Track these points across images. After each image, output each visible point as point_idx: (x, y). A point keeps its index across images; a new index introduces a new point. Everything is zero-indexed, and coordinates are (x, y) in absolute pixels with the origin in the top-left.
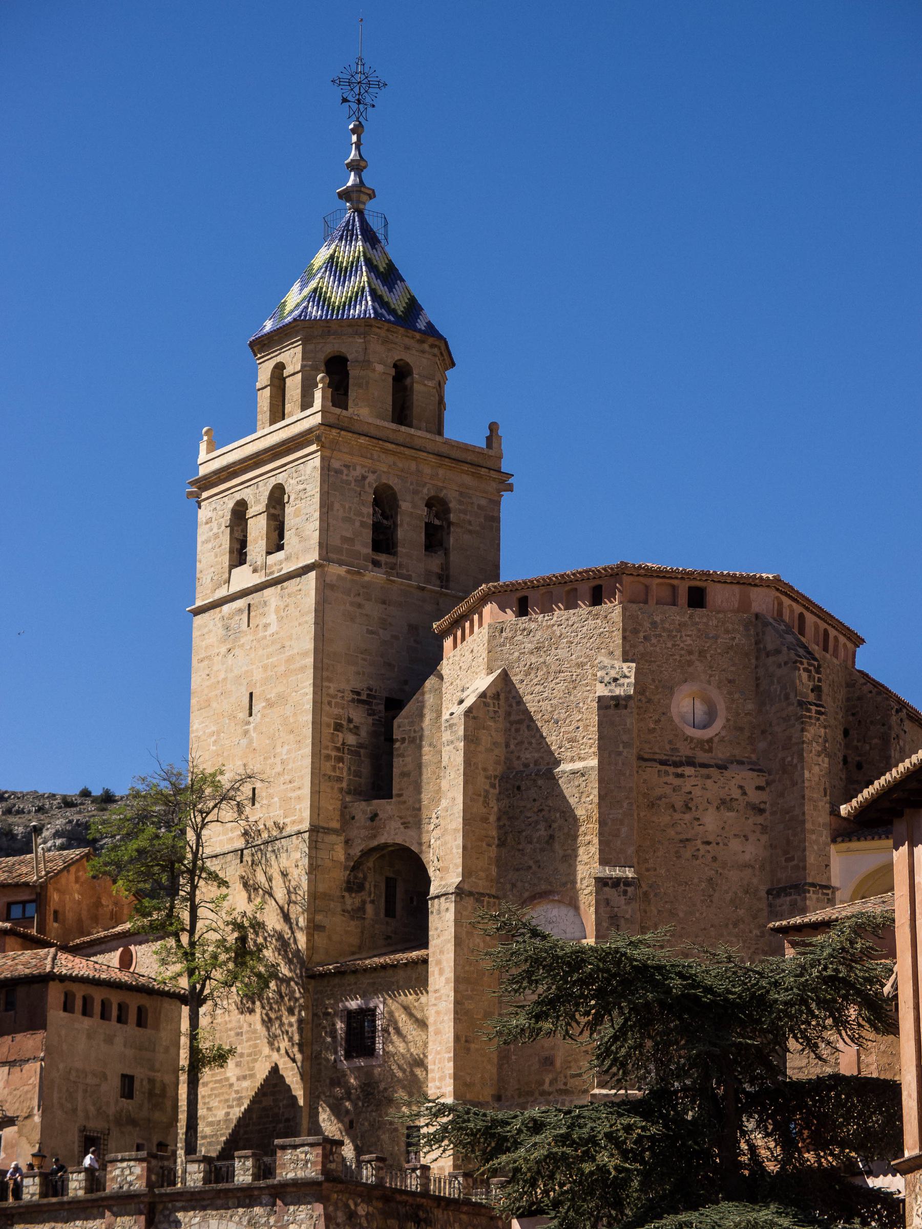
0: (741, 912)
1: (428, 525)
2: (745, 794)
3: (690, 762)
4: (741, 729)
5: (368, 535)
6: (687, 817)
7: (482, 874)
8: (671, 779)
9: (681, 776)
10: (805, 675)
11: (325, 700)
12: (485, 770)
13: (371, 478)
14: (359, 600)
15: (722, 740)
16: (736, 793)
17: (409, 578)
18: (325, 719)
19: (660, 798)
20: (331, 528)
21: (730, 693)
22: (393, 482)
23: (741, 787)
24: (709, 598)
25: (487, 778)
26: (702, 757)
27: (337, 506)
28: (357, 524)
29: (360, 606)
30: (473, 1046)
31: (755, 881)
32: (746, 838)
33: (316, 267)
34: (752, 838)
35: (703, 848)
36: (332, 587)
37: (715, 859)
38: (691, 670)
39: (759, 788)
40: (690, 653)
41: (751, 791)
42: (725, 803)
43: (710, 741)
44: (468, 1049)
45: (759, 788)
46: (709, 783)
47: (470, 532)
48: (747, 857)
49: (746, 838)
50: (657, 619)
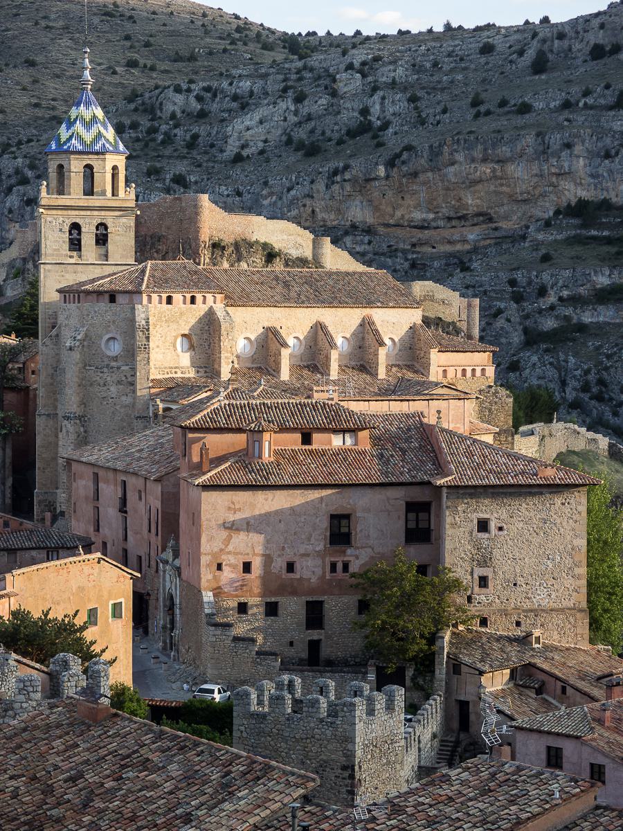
0: (125, 424)
1: (96, 235)
2: (127, 378)
3: (108, 366)
4: (129, 351)
5: (67, 246)
6: (105, 388)
7: (51, 406)
8: (99, 374)
9: (103, 372)
10: (141, 333)
11: (47, 317)
12: (51, 365)
13: (69, 222)
14: (62, 273)
15: (121, 356)
16: (124, 379)
17: (88, 260)
18: (47, 325)
19: (94, 382)
20: (48, 247)
21: (125, 337)
22: (77, 221)
23: (125, 376)
24: (117, 299)
25: (53, 368)
26: (114, 364)
27: (50, 236)
28: (61, 242)
29: (63, 276)
30: (46, 471)
31: (130, 412)
32: (127, 395)
33: (73, 118)
34: (129, 395)
35: (111, 400)
36: (49, 271)
37: (115, 404)
38: (110, 329)
39: (132, 376)
40: (109, 322)
41: (128, 375)
42: (119, 383)
43: (117, 357)
44: (44, 472)
45: (132, 376)
46: (113, 374)
47: (119, 235)
48: (127, 402)
49: (127, 395)
50: (97, 310)
